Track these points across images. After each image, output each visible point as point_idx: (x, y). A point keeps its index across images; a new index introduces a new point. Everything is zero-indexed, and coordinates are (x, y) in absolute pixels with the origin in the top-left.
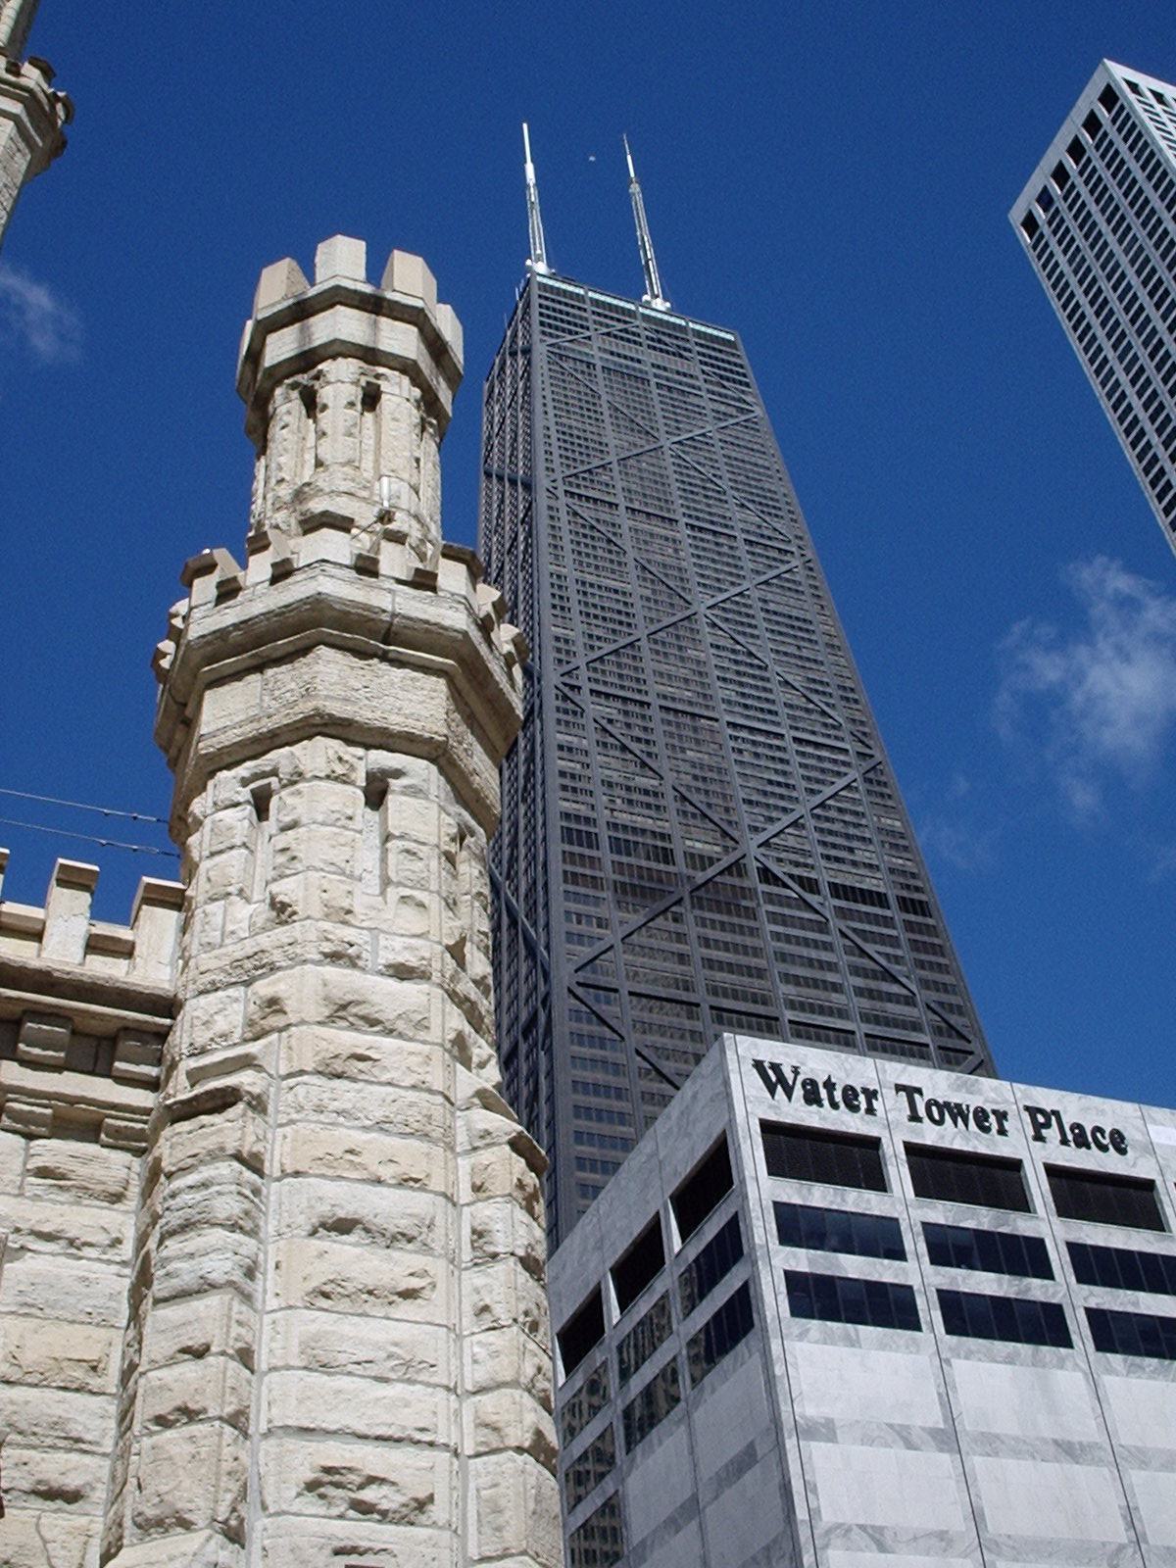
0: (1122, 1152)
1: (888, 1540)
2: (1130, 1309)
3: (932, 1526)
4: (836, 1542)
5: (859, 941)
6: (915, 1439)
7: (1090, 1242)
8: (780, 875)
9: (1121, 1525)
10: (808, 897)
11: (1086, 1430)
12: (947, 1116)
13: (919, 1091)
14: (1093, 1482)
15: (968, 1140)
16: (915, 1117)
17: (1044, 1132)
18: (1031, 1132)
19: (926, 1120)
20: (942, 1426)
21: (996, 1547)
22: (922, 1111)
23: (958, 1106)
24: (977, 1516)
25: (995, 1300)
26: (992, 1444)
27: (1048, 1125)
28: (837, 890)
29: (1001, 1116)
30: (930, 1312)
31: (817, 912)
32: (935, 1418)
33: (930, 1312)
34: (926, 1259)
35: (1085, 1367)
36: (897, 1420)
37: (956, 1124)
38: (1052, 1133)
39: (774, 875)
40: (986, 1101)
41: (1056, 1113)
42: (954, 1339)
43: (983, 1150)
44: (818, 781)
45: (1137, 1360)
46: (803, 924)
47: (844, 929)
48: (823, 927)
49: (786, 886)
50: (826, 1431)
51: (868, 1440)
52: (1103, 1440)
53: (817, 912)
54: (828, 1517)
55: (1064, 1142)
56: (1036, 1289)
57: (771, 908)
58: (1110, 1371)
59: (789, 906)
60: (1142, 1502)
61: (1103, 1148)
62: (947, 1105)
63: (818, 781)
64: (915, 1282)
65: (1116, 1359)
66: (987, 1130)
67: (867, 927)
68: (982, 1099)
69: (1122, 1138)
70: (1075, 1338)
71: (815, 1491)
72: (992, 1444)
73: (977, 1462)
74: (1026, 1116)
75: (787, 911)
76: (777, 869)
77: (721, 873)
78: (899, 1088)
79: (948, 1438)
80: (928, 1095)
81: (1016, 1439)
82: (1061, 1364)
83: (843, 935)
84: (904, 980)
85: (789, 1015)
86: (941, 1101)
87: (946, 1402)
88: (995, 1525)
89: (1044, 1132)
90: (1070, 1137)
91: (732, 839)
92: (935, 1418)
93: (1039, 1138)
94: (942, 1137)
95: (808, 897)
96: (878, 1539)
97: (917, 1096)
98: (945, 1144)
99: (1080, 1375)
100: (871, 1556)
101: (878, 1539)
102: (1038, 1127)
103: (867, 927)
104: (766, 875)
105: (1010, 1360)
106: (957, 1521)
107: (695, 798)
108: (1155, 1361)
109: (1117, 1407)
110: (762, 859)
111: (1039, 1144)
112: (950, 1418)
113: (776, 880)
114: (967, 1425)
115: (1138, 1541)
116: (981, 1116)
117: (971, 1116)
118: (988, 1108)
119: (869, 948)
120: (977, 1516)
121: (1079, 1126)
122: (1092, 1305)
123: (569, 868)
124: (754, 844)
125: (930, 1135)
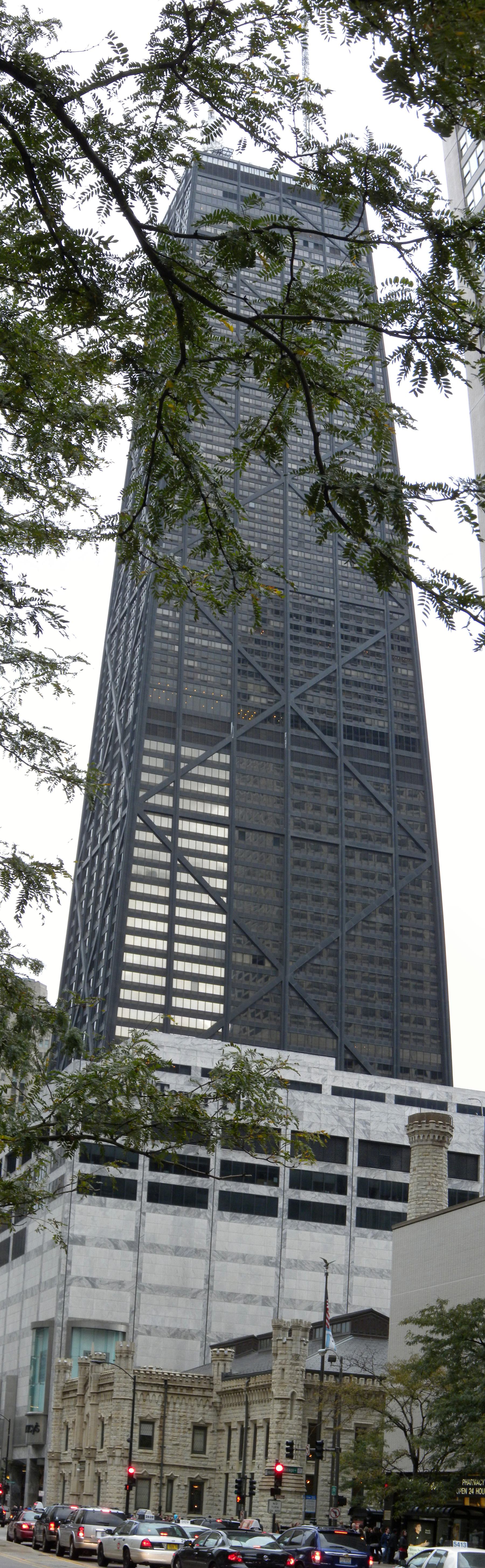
1: (97, 1282)
2: (243, 1191)
3: (119, 1278)
4: (75, 1283)
5: (358, 774)
6: (120, 1244)
7: (234, 1160)
8: (308, 721)
9: (203, 1282)
10: (328, 739)
11: (203, 1244)
14: (198, 1266)
20: (133, 1240)
21: (143, 1288)
24: (138, 1277)
25: (175, 1187)
26: (154, 1248)
28: (350, 733)
30: (142, 1192)
31: (330, 751)
32: (131, 1237)
33: (142, 1192)
34: (147, 1168)
35: (210, 1217)
36: (113, 1237)
39: (303, 721)
42: (150, 1204)
44: (353, 639)
45: (237, 1215)
46: (318, 761)
47: (349, 765)
48: (333, 762)
49: (310, 729)
50: (81, 1241)
51: (98, 1245)
52: (207, 1248)
53: (330, 751)
54: (74, 1273)
56: (199, 1182)
57: (295, 748)
58: (222, 1219)
59: (312, 747)
60: (217, 1275)
63: (353, 639)
64: (139, 1178)
65: (227, 1215)
67: (367, 762)
70: (210, 1204)
71: (70, 1264)
72: (154, 1248)
73: (146, 1256)
75: (307, 751)
77: (265, 721)
79: (135, 1246)
81: (166, 1247)
82: (199, 1216)
83: (346, 768)
85: (293, 832)
87: (138, 1231)
88: (148, 1278)
92: (131, 1237)
95: (328, 739)
96: (93, 1283)
97: (166, 1088)
99: (206, 1221)
100: (88, 1289)
101: (93, 1283)
103: (367, 762)
104: (297, 721)
105: (175, 1213)
106: (128, 1277)
107: (254, 659)
108: (246, 1216)
109: (220, 1235)
110: (296, 708)
112: (138, 1236)
114: (146, 1239)
115: (209, 1289)
119: (364, 778)
120: (138, 1277)
122: (224, 1189)
123: (152, 721)
124: (292, 696)
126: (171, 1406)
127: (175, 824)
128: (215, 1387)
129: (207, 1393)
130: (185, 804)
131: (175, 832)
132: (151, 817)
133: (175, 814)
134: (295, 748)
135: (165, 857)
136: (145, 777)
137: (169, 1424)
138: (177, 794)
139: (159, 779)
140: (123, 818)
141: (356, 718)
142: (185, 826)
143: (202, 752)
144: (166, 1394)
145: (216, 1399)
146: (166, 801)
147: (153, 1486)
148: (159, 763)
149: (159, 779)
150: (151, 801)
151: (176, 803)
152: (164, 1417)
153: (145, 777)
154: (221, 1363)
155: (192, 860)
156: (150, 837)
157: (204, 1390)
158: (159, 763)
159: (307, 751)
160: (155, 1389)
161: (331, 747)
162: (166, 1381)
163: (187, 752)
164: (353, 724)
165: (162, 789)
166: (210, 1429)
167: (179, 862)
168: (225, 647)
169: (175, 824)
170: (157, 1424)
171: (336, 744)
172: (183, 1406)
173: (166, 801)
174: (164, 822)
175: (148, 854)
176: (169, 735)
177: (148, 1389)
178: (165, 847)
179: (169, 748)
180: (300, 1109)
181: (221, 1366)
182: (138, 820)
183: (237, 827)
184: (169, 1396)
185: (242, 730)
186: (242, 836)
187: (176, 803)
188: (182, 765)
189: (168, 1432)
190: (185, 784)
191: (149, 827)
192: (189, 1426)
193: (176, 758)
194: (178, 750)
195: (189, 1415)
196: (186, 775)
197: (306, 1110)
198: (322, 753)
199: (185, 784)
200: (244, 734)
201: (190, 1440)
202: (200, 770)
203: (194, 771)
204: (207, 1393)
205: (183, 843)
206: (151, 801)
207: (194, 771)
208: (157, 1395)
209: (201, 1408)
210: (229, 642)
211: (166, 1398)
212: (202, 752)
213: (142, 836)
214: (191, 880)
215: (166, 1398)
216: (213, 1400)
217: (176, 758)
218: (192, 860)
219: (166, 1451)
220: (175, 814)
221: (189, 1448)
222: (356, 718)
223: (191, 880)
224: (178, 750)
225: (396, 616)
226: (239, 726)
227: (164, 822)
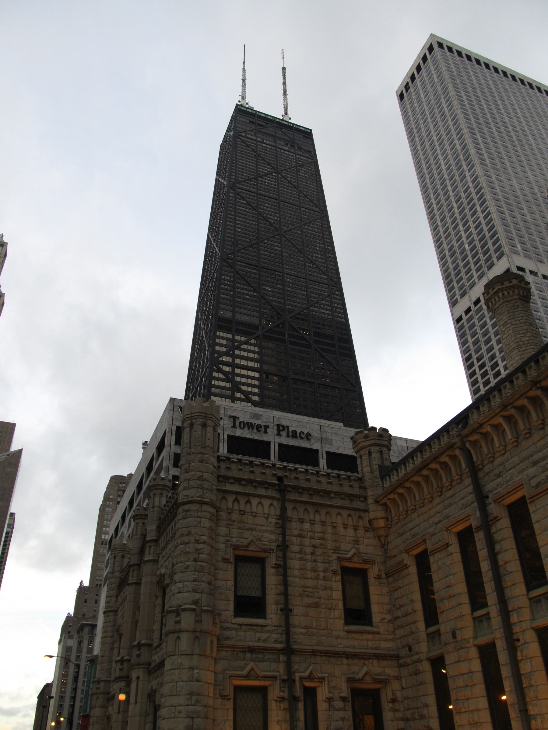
0: (309, 439)
12: (246, 428)
13: (238, 418)
15: (252, 435)
16: (234, 426)
17: (281, 433)
18: (276, 432)
19: (238, 428)
22: (237, 424)
23: (251, 423)
27: (284, 430)
29: (266, 427)
31: (307, 341)
37: (249, 429)
38: (284, 433)
40: (262, 422)
41: (288, 427)
43: (256, 438)
53: (307, 341)
55: (288, 436)
57: (291, 339)
61: (301, 438)
62: (247, 423)
66: (259, 431)
67: (325, 347)
68: (261, 421)
69: (310, 435)
74: (276, 428)
75: (297, 341)
76: (295, 326)
78: (230, 417)
80: (241, 419)
83: (316, 349)
84: (335, 366)
86: (245, 422)
89: (281, 433)
90: (290, 435)
91: (281, 315)
93: (279, 434)
94: (243, 434)
98: (244, 436)
102: (279, 431)
103: (325, 347)
111: (278, 437)
113: (294, 329)
116: (259, 427)
117: (255, 427)
118: (262, 424)
121: (296, 432)
125: (238, 433)
126: (294, 525)
127: (233, 370)
128: (370, 493)
129: (359, 505)
130: (238, 361)
131: (234, 374)
132: (221, 366)
133: (233, 365)
134: (291, 339)
135: (229, 385)
136: (217, 348)
137: (295, 564)
138: (234, 356)
139: (225, 349)
140: (206, 369)
141: (319, 328)
142: (238, 371)
143: (246, 339)
144: (283, 501)
145: (376, 512)
146: (228, 359)
147: (273, 705)
148: (225, 342)
149: (225, 349)
150: (221, 359)
151: (233, 360)
152: (284, 547)
153: (217, 348)
154: (374, 449)
155: (242, 387)
156: (220, 375)
157: (352, 497)
158: (225, 342)
159: (297, 341)
160: (261, 491)
161: (308, 339)
162: (280, 479)
163: (238, 338)
164: (318, 330)
165: (226, 354)
166: (373, 573)
167: (236, 387)
168: (255, 294)
169: (233, 370)
170: (272, 560)
171: (310, 339)
172: (318, 528)
173: (228, 359)
174: (228, 369)
175: (220, 383)
176: (227, 330)
177: (249, 490)
178: (228, 380)
179: (229, 336)
180: (330, 437)
181: (375, 455)
182: (214, 367)
183: (264, 373)
184: (289, 506)
185: (265, 330)
186: (267, 377)
187: (233, 360)
188: (236, 344)
189: (295, 580)
190: (238, 352)
191: (220, 371)
192: (335, 566)
193: (233, 340)
194: (234, 337)
195: (330, 545)
196: (238, 348)
197: (333, 438)
198: (304, 342)
199: (238, 352)
200: (266, 332)
201: (337, 595)
202: (246, 347)
203: (242, 347)
204: (359, 505)
205: (238, 379)
206: (221, 359)
207: (242, 347)
208: (266, 503)
209: (351, 532)
210: (257, 292)
211: (283, 509)
212: (246, 339)
213: (216, 374)
214: (242, 396)
215: (283, 509)
216: (372, 515)
217: (233, 340)
218: (242, 387)
219: (294, 620)
220: (233, 365)
221: (339, 612)
222: (319, 328)
223: (242, 396)
224: (234, 337)
225: (334, 288)
226: (263, 328)
227: (228, 369)
